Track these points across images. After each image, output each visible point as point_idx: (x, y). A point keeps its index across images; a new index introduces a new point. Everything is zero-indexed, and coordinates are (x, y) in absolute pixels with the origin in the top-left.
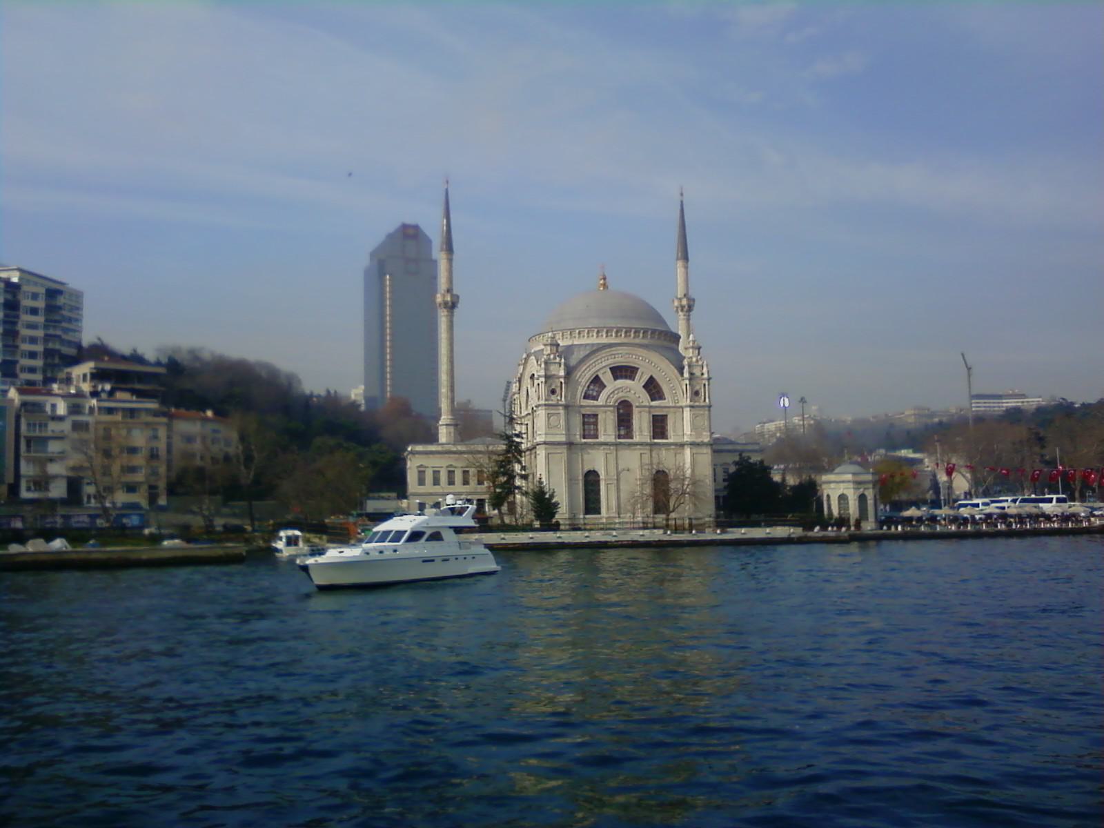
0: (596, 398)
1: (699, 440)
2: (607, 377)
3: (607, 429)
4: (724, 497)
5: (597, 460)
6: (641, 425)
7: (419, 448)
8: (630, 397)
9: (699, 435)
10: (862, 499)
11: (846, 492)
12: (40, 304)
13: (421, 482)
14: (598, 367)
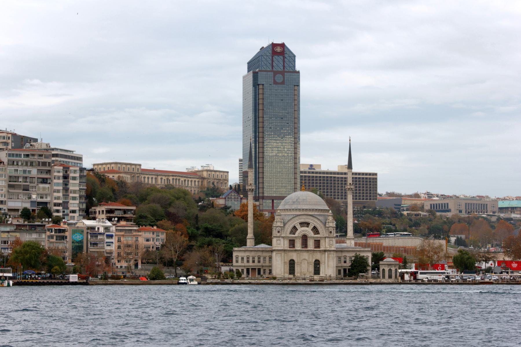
0: (294, 234)
1: (331, 249)
2: (298, 226)
3: (298, 245)
4: (349, 269)
5: (294, 256)
7: (236, 249)
8: (306, 233)
9: (330, 247)
10: (390, 270)
11: (385, 268)
12: (77, 175)
13: (237, 262)
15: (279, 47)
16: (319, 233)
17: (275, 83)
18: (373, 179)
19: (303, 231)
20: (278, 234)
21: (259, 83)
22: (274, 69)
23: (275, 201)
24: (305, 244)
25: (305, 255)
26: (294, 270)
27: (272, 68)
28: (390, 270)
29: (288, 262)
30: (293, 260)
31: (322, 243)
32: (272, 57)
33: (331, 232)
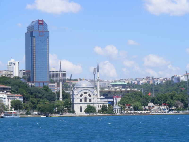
2: (83, 94)
3: (83, 101)
6: (88, 101)
15: (41, 21)
16: (91, 96)
17: (40, 36)
18: (65, 73)
20: (76, 97)
21: (33, 36)
22: (39, 30)
23: (40, 83)
24: (86, 101)
25: (86, 105)
26: (82, 111)
27: (39, 30)
28: (118, 110)
29: (80, 107)
30: (81, 107)
31: (92, 100)
32: (39, 25)
33: (95, 96)
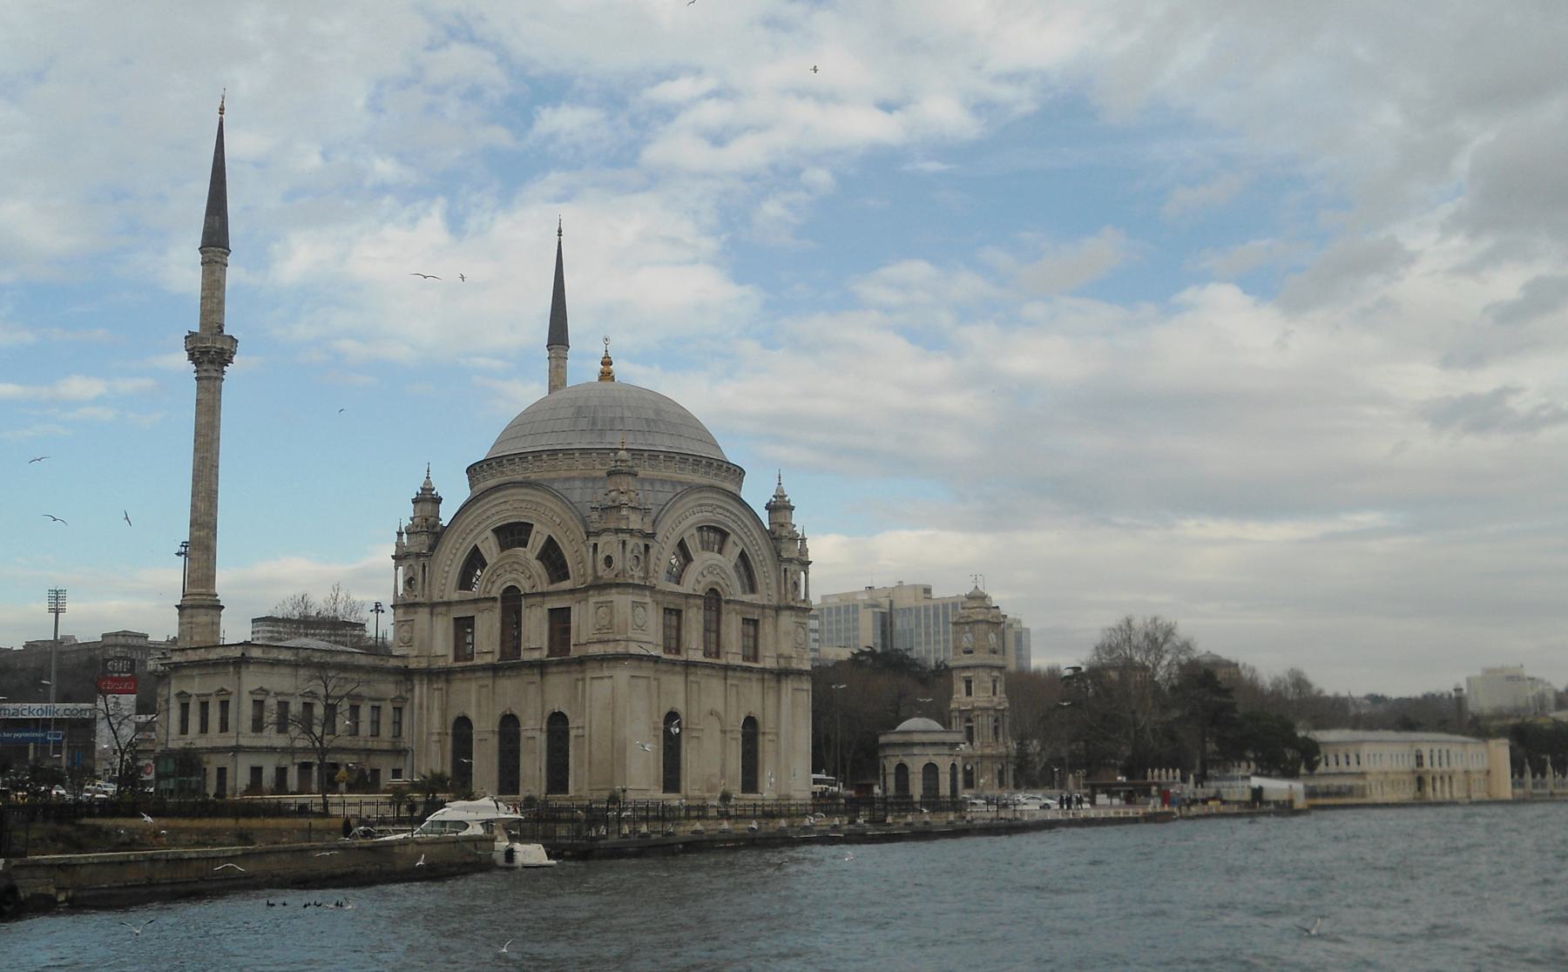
2: (693, 545)
11: (938, 761)
14: (686, 524)
19: (711, 569)
25: (712, 693)
31: (766, 628)
